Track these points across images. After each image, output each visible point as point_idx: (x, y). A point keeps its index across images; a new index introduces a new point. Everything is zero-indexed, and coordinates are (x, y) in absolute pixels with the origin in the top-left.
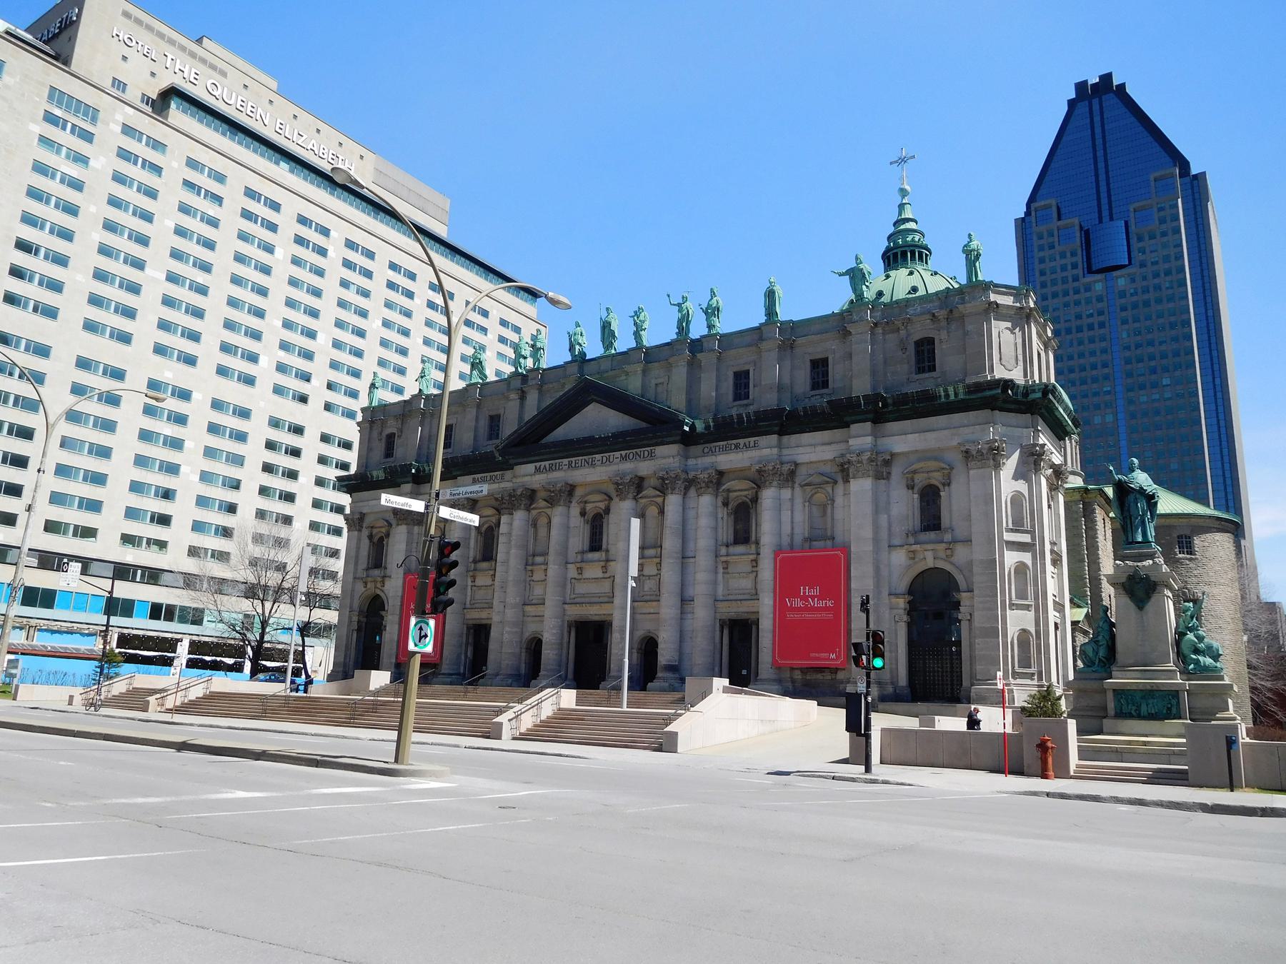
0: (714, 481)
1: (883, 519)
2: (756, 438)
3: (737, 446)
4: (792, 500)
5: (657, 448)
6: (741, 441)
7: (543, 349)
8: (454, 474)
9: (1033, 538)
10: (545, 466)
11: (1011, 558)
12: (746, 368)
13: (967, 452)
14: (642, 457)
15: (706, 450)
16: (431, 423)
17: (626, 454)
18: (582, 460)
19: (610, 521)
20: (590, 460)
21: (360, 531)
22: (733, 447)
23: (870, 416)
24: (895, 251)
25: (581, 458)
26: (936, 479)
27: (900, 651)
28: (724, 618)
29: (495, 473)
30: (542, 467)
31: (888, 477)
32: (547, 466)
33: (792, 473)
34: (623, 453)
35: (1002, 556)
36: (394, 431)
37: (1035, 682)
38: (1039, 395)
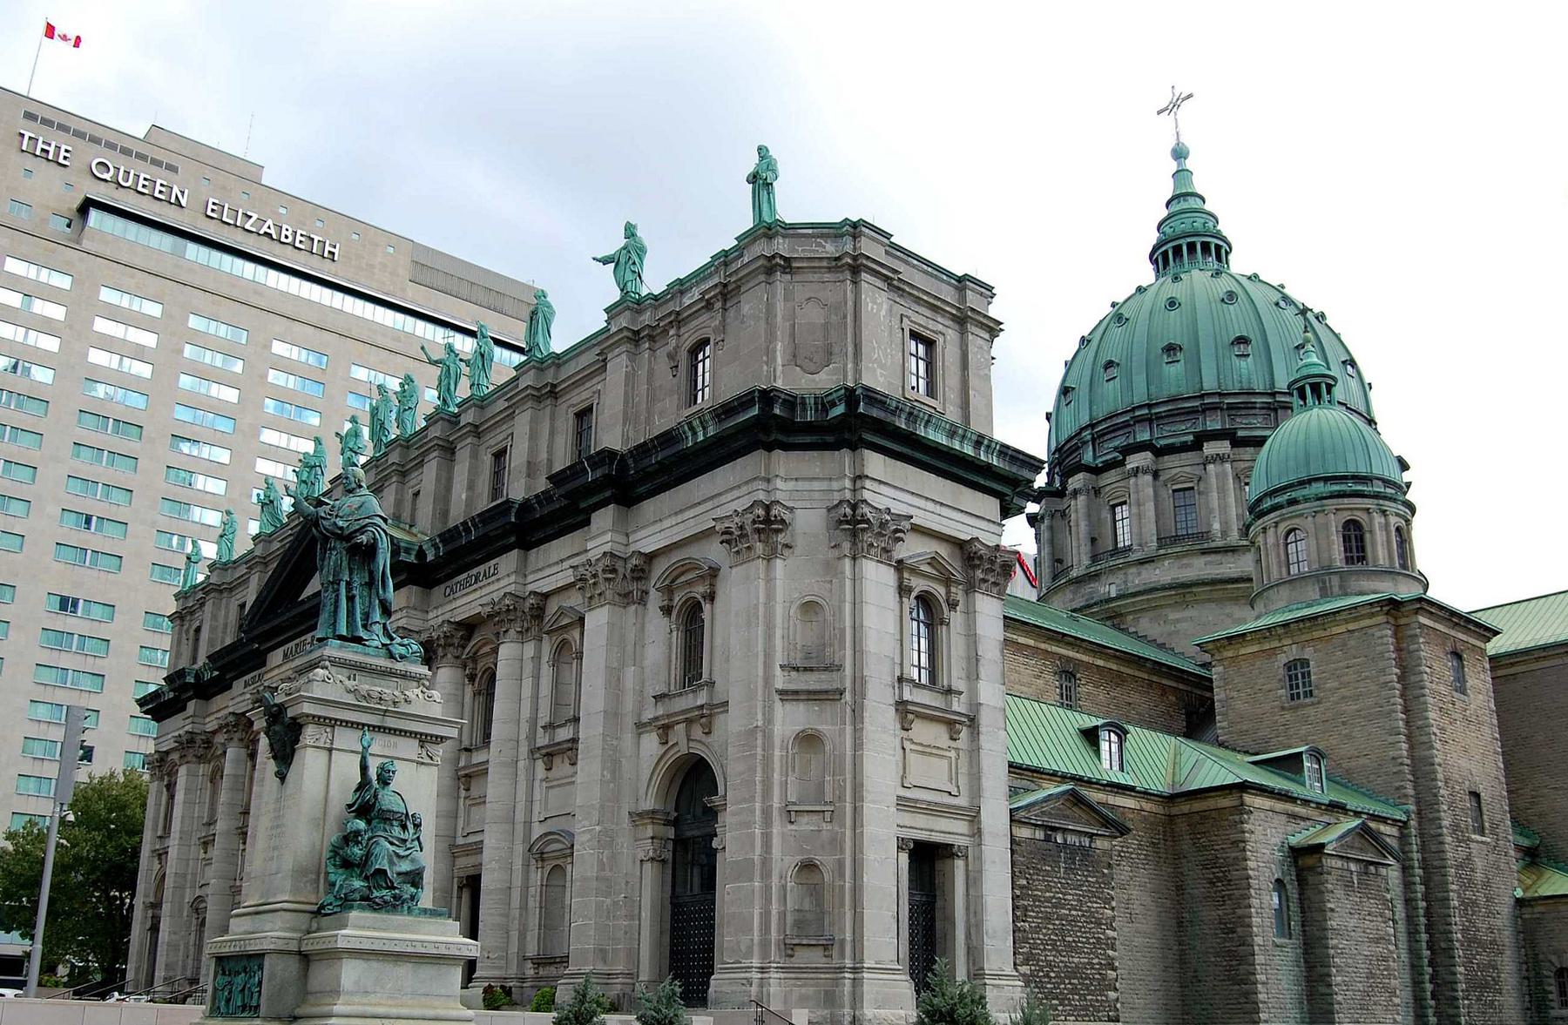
0: (456, 641)
1: (630, 673)
4: (537, 658)
6: (481, 568)
7: (320, 466)
9: (842, 679)
11: (789, 720)
12: (503, 445)
13: (727, 532)
15: (448, 590)
16: (227, 607)
21: (162, 779)
23: (608, 494)
24: (1164, 249)
26: (699, 590)
27: (643, 914)
28: (462, 874)
31: (643, 600)
33: (538, 613)
35: (769, 720)
36: (197, 624)
37: (836, 962)
38: (840, 410)
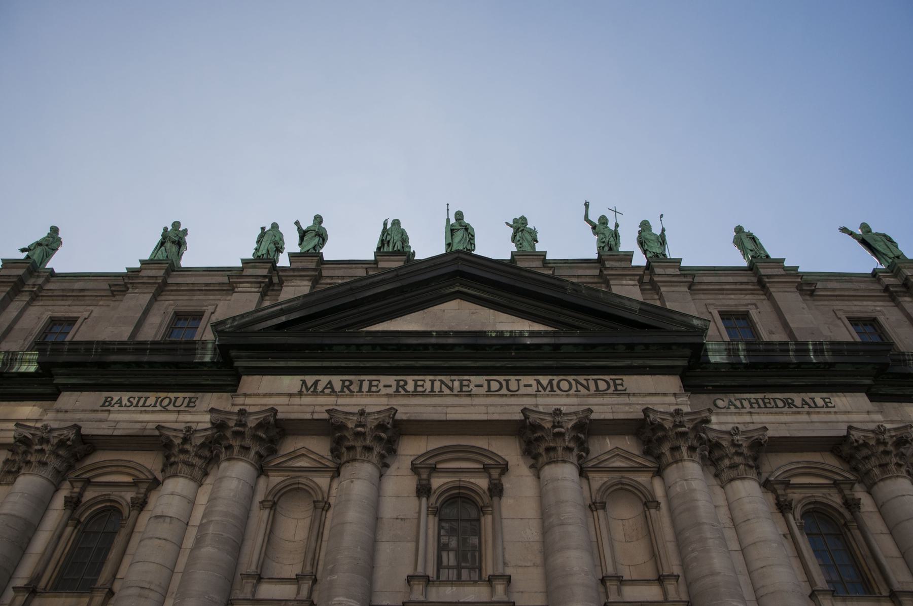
2: (824, 395)
3: (789, 404)
5: (625, 378)
8: (58, 380)
10: (330, 383)
14: (592, 387)
17: (551, 382)
18: (433, 382)
19: (505, 513)
20: (456, 384)
22: (780, 404)
25: (432, 377)
29: (172, 395)
30: (320, 388)
32: (337, 386)
34: (544, 380)
